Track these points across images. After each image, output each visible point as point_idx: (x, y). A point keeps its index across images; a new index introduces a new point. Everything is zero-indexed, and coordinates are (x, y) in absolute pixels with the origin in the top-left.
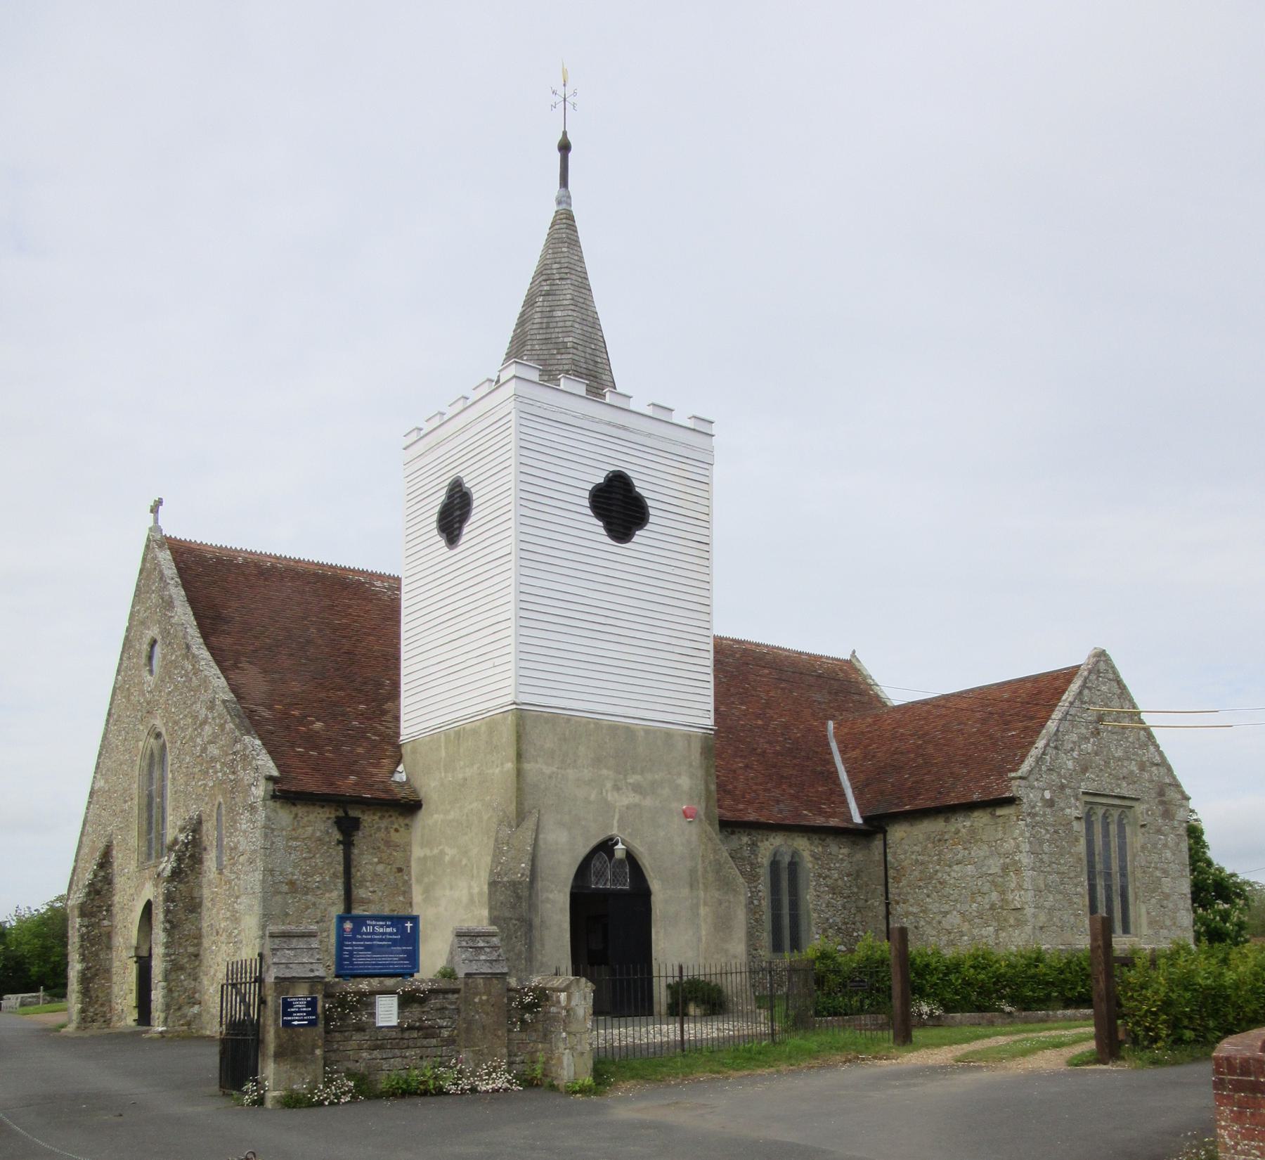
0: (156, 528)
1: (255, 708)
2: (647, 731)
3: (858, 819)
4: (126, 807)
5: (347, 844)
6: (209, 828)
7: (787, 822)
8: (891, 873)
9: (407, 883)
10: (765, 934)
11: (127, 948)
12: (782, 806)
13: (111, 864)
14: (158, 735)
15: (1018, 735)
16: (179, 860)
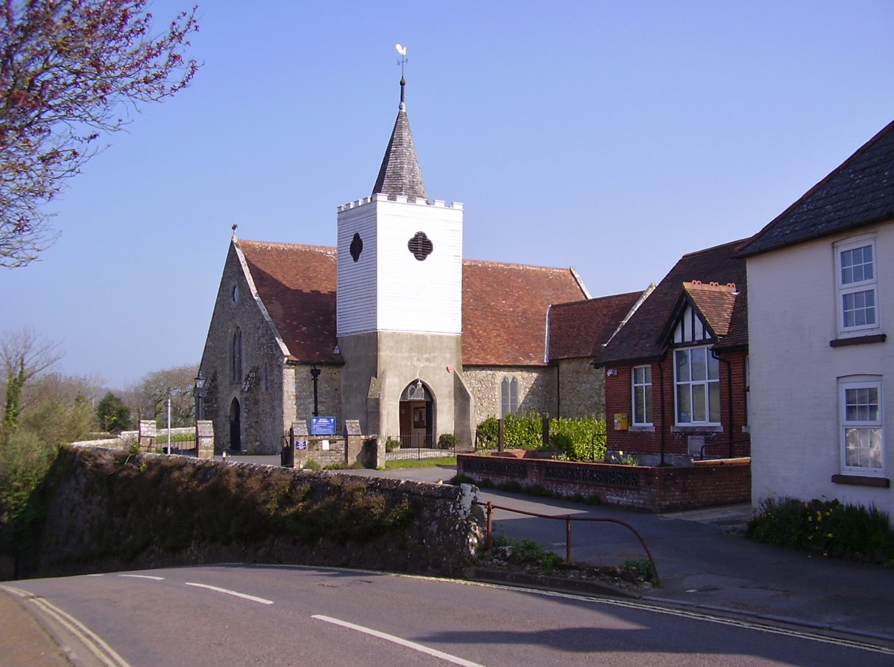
2: (432, 336)
5: (315, 380)
7: (510, 364)
8: (560, 385)
10: (498, 414)
13: (217, 380)
14: (238, 328)
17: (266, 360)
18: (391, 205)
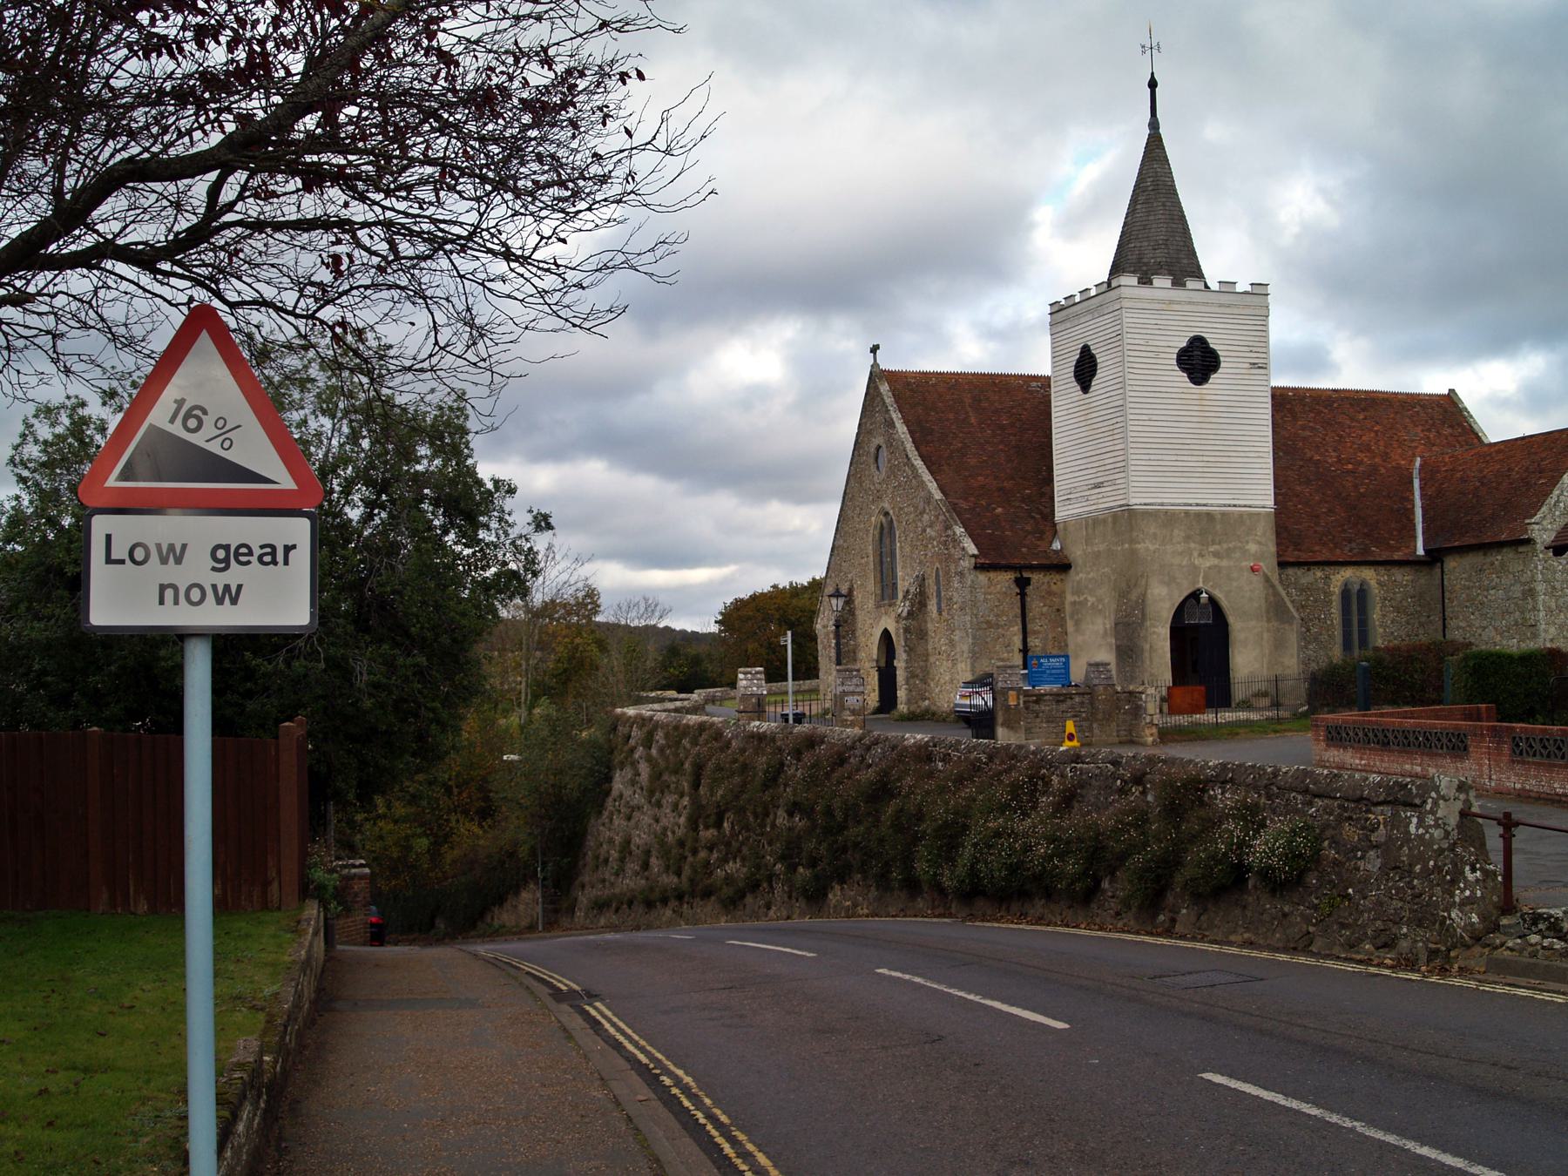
0: (875, 365)
1: (956, 501)
3: (1420, 551)
4: (863, 561)
5: (1023, 595)
6: (931, 582)
8: (1447, 594)
9: (1063, 619)
11: (869, 661)
12: (1354, 545)
13: (853, 601)
14: (886, 514)
15: (1545, 483)
16: (912, 605)
17: (937, 565)
18: (1145, 292)
